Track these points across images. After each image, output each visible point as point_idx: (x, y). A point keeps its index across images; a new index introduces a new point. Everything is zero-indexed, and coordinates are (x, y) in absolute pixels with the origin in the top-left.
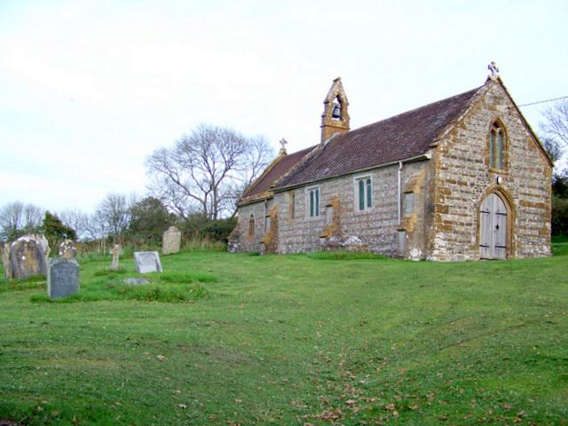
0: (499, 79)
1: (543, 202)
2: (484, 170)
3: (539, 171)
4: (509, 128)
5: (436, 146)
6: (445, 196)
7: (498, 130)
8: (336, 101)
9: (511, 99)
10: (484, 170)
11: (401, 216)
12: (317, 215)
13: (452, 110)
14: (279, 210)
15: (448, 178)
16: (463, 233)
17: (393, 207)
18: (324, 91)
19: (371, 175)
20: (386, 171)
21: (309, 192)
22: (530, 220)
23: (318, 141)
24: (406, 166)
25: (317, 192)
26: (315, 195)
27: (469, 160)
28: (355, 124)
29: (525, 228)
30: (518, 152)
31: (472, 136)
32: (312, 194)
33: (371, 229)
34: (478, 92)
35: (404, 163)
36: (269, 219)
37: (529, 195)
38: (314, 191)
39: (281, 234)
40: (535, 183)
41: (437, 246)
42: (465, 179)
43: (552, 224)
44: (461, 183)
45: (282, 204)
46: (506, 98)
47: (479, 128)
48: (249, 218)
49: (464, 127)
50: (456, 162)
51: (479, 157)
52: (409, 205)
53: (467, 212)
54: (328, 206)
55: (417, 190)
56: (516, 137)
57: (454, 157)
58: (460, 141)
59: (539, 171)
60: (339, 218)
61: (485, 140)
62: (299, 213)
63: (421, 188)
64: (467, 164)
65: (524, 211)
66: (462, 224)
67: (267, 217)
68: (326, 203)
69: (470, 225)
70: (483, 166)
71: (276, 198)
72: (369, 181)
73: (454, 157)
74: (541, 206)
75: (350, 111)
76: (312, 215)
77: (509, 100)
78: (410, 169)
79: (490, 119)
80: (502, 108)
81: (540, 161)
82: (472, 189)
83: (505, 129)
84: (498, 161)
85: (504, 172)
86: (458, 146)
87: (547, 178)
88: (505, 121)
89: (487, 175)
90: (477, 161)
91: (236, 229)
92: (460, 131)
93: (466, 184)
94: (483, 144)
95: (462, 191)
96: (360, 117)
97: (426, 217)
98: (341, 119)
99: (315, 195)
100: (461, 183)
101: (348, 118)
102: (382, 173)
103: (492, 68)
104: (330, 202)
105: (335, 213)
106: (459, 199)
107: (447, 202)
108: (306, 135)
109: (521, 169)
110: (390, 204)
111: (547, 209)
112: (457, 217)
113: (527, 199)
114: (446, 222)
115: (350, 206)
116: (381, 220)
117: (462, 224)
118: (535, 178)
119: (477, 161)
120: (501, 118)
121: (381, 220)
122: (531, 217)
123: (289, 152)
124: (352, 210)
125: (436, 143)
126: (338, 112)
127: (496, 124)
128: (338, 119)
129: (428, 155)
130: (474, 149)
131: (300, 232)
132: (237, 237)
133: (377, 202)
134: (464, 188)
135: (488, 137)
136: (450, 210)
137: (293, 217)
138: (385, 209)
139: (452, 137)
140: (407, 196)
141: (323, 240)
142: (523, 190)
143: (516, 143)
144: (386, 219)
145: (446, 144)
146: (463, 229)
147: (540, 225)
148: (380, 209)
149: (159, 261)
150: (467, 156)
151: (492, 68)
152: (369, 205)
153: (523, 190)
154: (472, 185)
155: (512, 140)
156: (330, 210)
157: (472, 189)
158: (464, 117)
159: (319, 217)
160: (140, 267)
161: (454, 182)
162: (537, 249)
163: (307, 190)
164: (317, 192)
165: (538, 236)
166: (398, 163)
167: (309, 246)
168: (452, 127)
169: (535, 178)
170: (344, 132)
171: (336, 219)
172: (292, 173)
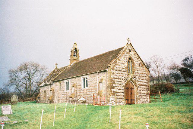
0: (131, 44)
1: (147, 84)
2: (126, 74)
3: (145, 74)
4: (134, 60)
5: (110, 67)
6: (113, 83)
7: (130, 61)
8: (75, 51)
9: (135, 50)
10: (126, 74)
11: (98, 90)
12: (69, 90)
13: (116, 53)
14: (55, 88)
15: (114, 77)
16: (120, 96)
17: (96, 87)
18: (72, 47)
19: (88, 76)
20: (93, 75)
21: (66, 82)
22: (142, 91)
23: (69, 64)
24: (100, 73)
25: (69, 82)
26: (68, 83)
27: (121, 71)
28: (81, 59)
29: (141, 93)
30: (138, 69)
31: (123, 59)
32: (67, 82)
33: (88, 95)
34: (124, 48)
35: (99, 72)
36: (51, 91)
37: (141, 82)
38: (68, 82)
39: (55, 96)
40: (144, 78)
41: (110, 100)
42: (120, 77)
43: (150, 91)
44: (119, 79)
45: (56, 86)
46: (133, 49)
47: (124, 60)
48: (44, 91)
49: (119, 60)
50: (117, 72)
51: (124, 70)
52: (101, 86)
53: (121, 88)
54: (72, 87)
55: (104, 81)
56: (137, 62)
57: (116, 70)
58: (118, 65)
59: (145, 74)
60: (76, 91)
61: (126, 64)
62: (60, 89)
63: (105, 81)
64: (120, 72)
65: (140, 87)
66: (119, 93)
67: (50, 91)
68: (72, 86)
69: (122, 92)
70: (126, 73)
71: (54, 84)
72: (87, 78)
73: (116, 70)
74: (146, 85)
75: (80, 54)
76: (67, 90)
77: (134, 51)
78: (101, 74)
79: (128, 57)
80: (132, 53)
81: (145, 70)
82: (122, 81)
83: (133, 60)
84: (130, 71)
85: (133, 74)
86: (117, 66)
87: (148, 76)
88: (133, 58)
89: (127, 76)
90: (124, 71)
91: (39, 95)
92: (118, 61)
93: (120, 79)
94: (126, 65)
95: (119, 81)
96: (83, 56)
97: (107, 90)
98: (77, 57)
99: (68, 83)
100: (119, 79)
101: (79, 56)
102: (91, 75)
103: (128, 40)
104: (73, 86)
105: (75, 89)
106: (118, 84)
107: (114, 85)
108: (65, 62)
109: (139, 73)
110: (95, 86)
111: (148, 86)
112: (117, 90)
113: (141, 83)
114: (114, 92)
115: (80, 87)
116: (91, 91)
117: (119, 93)
118: (144, 76)
119: (124, 71)
120: (131, 57)
121: (91, 91)
122: (143, 89)
123: (58, 68)
124: (81, 88)
125: (110, 66)
126: (75, 54)
127: (130, 59)
128: (75, 57)
129: (107, 70)
130: (123, 67)
131: (63, 96)
132: (39, 98)
133: (90, 85)
134: (120, 80)
135: (127, 63)
136: (115, 88)
137: (60, 90)
138: (93, 88)
139: (115, 63)
140: (100, 83)
141: (71, 99)
142: (139, 80)
143: (137, 65)
144: (93, 91)
145: (113, 66)
146: (120, 94)
147: (146, 92)
148: (91, 88)
149: (11, 109)
150: (120, 70)
151: (128, 40)
152: (87, 86)
153: (139, 80)
154: (122, 79)
155: (135, 64)
156: (73, 88)
157: (122, 81)
158: (119, 56)
159: (69, 91)
160: (3, 111)
161: (116, 78)
162: (146, 100)
163: (65, 81)
164: (69, 82)
165: (146, 96)
166: (97, 72)
167: (66, 101)
168: (115, 60)
169: (144, 76)
170: (78, 61)
171: (76, 91)
172: (59, 76)
